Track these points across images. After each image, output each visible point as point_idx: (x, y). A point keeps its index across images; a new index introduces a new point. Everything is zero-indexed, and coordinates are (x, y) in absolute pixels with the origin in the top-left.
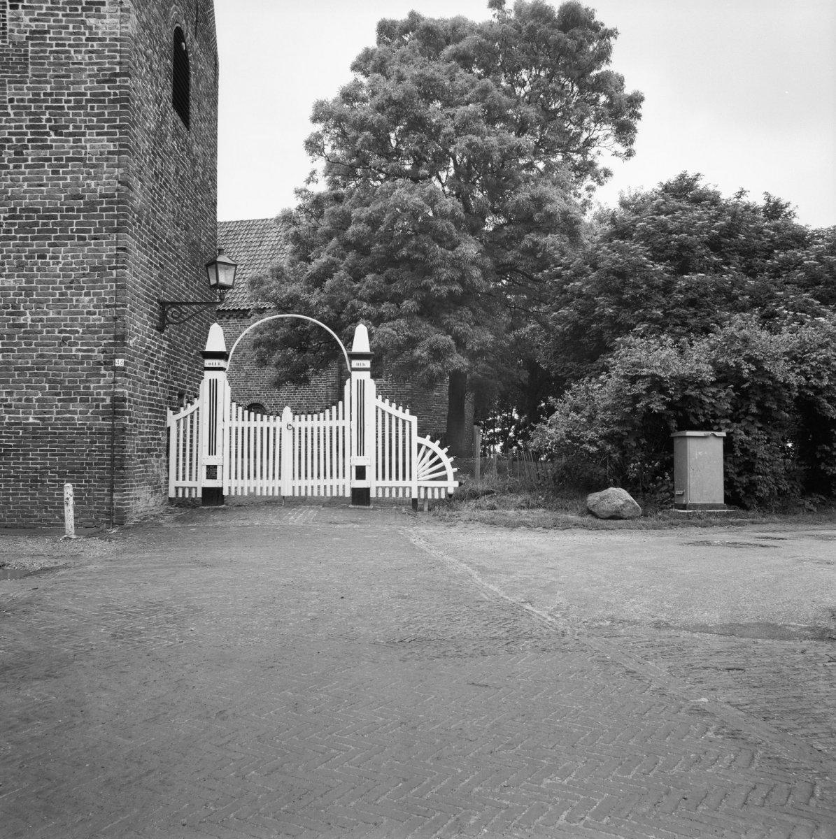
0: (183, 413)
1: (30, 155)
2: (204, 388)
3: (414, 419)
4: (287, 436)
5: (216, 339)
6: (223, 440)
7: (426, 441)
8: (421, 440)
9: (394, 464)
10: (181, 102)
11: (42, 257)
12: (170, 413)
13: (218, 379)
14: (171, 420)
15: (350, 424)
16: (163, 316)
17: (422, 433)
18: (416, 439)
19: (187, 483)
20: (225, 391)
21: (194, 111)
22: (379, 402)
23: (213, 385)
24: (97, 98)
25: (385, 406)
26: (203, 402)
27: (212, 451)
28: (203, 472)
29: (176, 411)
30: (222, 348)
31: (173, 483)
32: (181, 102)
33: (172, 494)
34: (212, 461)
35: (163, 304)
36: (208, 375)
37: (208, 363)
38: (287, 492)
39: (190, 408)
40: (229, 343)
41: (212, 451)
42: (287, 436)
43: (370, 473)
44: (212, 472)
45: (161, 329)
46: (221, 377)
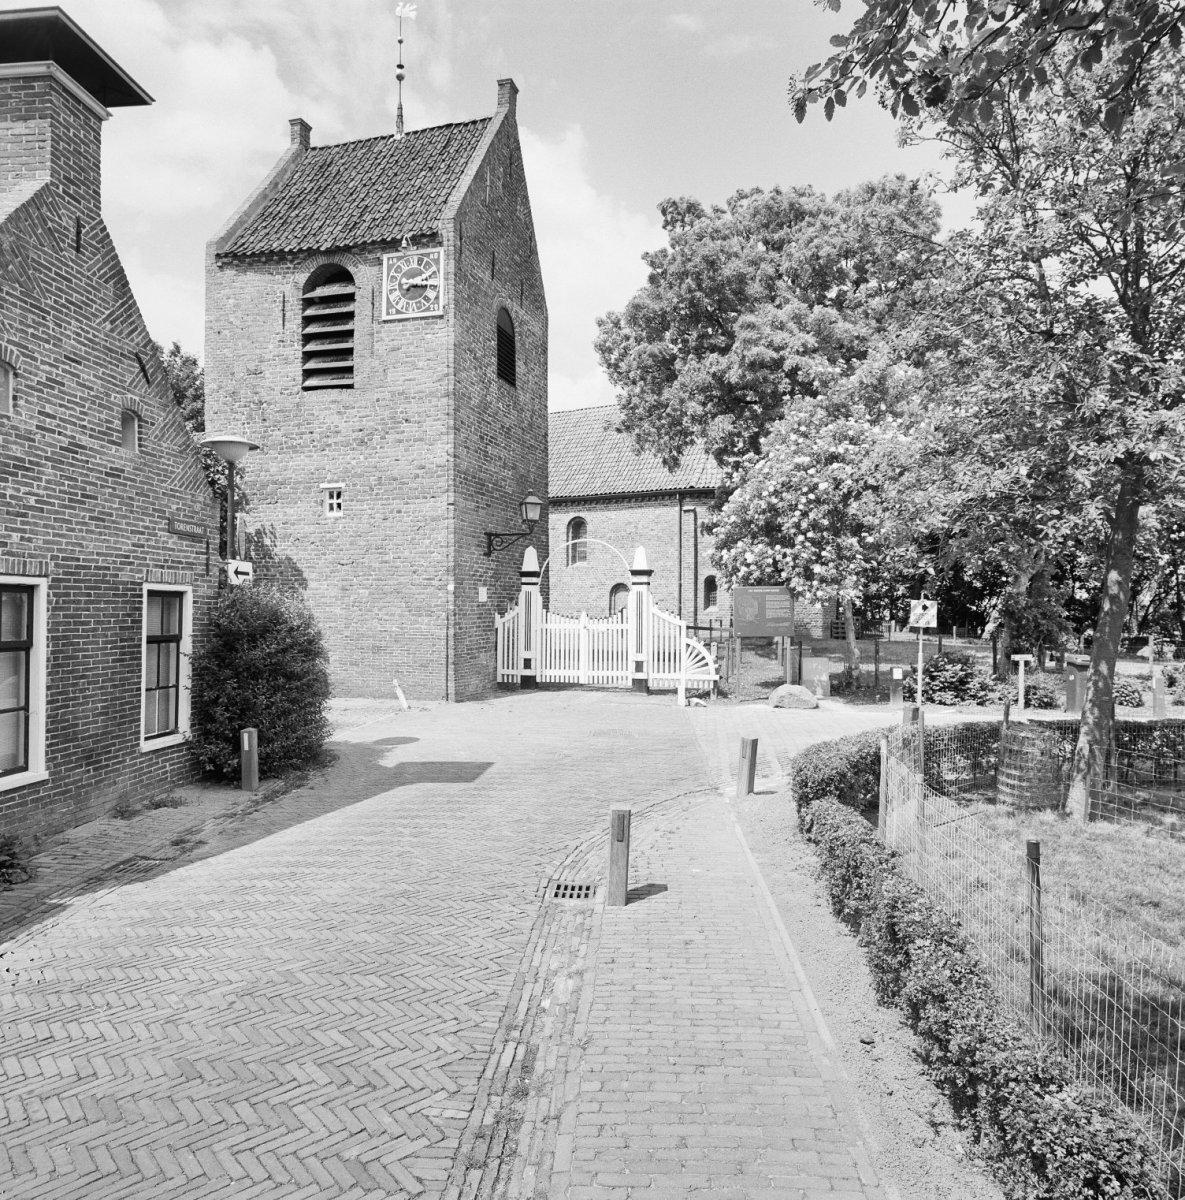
2: (522, 597)
8: (689, 641)
10: (506, 371)
11: (399, 512)
12: (497, 616)
14: (499, 621)
16: (490, 544)
19: (510, 672)
21: (520, 368)
22: (655, 609)
23: (528, 595)
26: (521, 609)
28: (521, 664)
29: (502, 614)
30: (537, 569)
31: (501, 671)
32: (506, 371)
33: (499, 680)
35: (489, 535)
37: (524, 580)
41: (528, 647)
42: (583, 633)
44: (527, 663)
45: (488, 554)
46: (535, 591)
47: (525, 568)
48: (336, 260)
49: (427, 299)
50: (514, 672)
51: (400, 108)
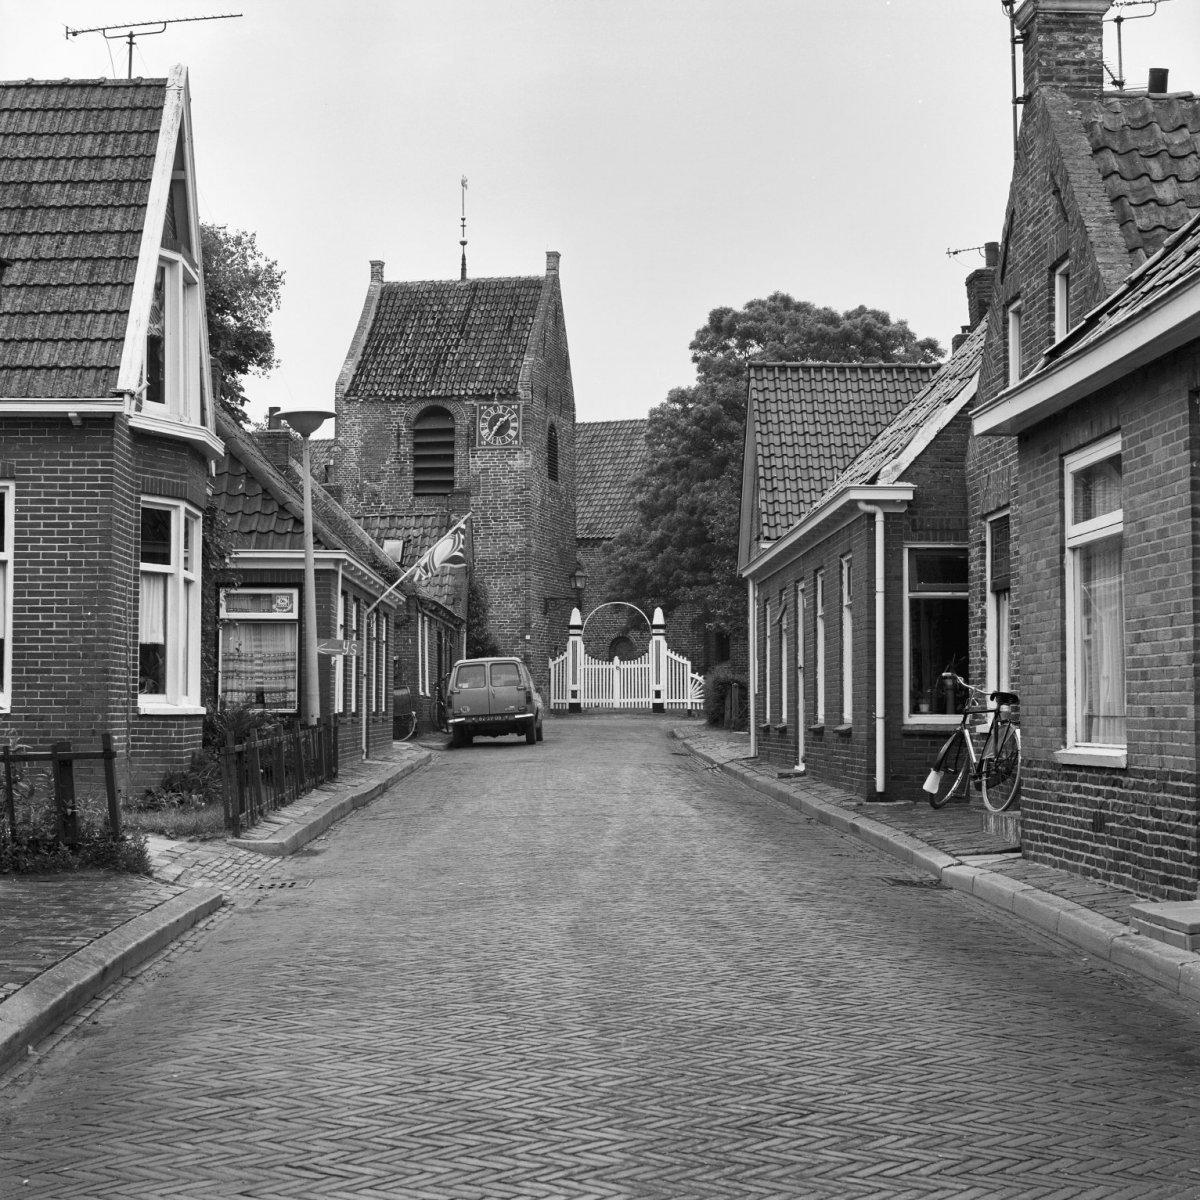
0: (558, 660)
1: (482, 533)
2: (570, 646)
3: (689, 663)
4: (616, 673)
5: (576, 618)
6: (580, 675)
7: (696, 676)
9: (677, 687)
13: (577, 641)
14: (551, 664)
15: (652, 666)
17: (693, 672)
18: (690, 675)
20: (581, 647)
23: (575, 644)
24: (514, 502)
25: (672, 655)
26: (569, 654)
27: (574, 682)
28: (569, 694)
29: (554, 659)
31: (553, 701)
33: (552, 707)
34: (574, 688)
35: (546, 599)
36: (572, 638)
37: (572, 631)
38: (617, 705)
39: (562, 658)
40: (583, 620)
41: (574, 682)
42: (616, 673)
43: (664, 695)
44: (574, 694)
45: (545, 614)
46: (579, 639)
47: (572, 623)
48: (440, 403)
49: (510, 436)
50: (564, 701)
51: (464, 256)
